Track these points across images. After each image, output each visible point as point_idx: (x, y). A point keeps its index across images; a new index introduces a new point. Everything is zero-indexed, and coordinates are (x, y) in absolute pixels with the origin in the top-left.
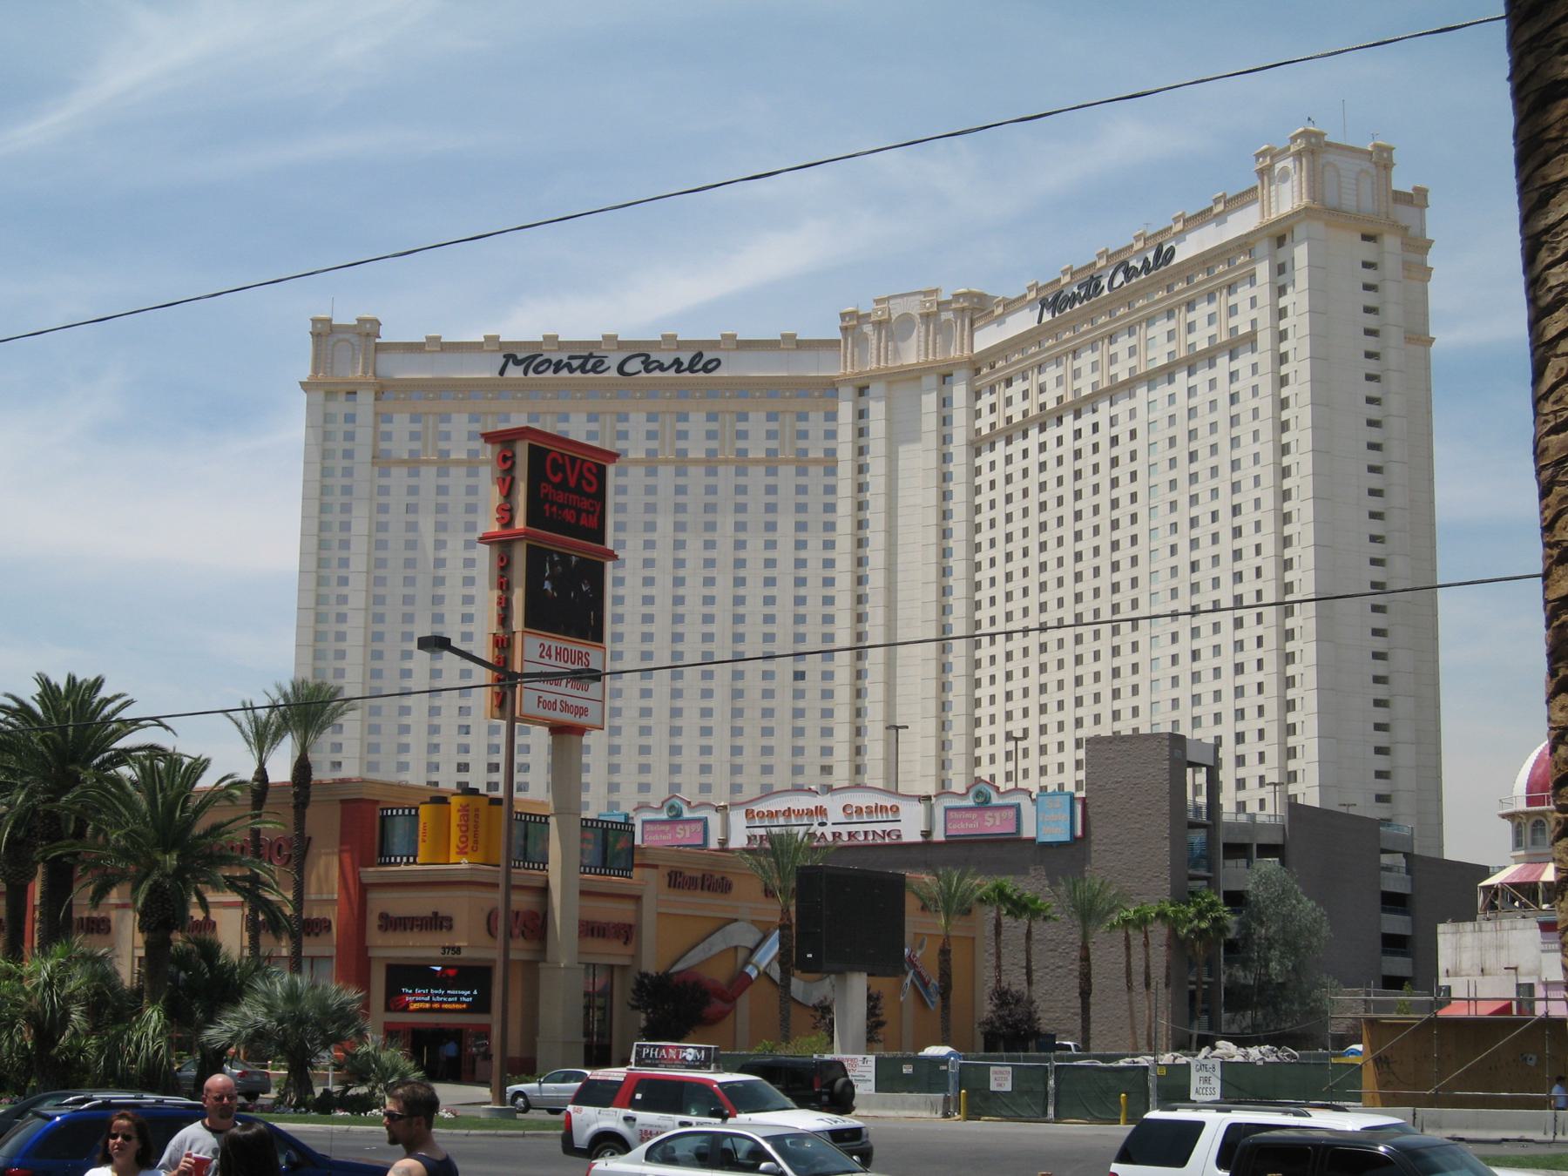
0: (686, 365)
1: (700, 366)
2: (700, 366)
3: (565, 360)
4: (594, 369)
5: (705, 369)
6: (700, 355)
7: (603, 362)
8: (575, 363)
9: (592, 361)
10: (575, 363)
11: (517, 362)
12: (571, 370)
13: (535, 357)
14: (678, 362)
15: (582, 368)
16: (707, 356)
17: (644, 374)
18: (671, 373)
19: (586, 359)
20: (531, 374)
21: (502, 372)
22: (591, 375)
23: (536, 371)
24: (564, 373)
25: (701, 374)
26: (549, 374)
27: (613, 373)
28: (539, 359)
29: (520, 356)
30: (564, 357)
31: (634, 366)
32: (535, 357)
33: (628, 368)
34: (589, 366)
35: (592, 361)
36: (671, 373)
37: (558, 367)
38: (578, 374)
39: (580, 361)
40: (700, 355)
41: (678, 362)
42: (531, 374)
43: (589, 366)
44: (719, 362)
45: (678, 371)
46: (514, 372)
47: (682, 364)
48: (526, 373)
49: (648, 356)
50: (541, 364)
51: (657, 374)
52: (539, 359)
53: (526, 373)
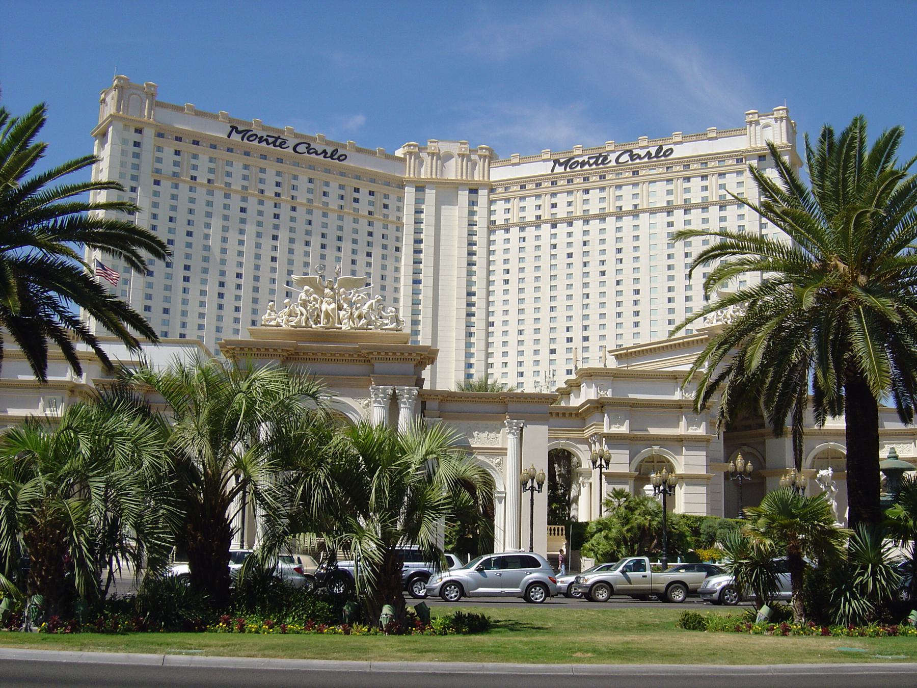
0: (653, 155)
1: (662, 154)
2: (662, 154)
3: (586, 160)
4: (603, 163)
5: (664, 155)
6: (661, 148)
7: (607, 159)
8: (592, 161)
9: (601, 159)
10: (592, 161)
11: (560, 165)
12: (590, 165)
13: (569, 160)
14: (649, 153)
15: (596, 163)
16: (665, 148)
17: (630, 162)
18: (646, 160)
19: (597, 158)
20: (568, 169)
21: (552, 171)
22: (601, 166)
23: (570, 168)
24: (587, 167)
25: (663, 158)
26: (579, 168)
27: (613, 163)
28: (573, 161)
29: (562, 161)
30: (586, 158)
31: (625, 158)
32: (569, 160)
33: (620, 161)
34: (600, 162)
35: (601, 159)
36: (646, 160)
37: (583, 164)
38: (594, 166)
39: (594, 160)
40: (661, 148)
41: (649, 153)
42: (568, 169)
43: (600, 162)
44: (672, 150)
45: (649, 158)
46: (559, 169)
47: (651, 154)
48: (565, 169)
49: (631, 151)
50: (574, 163)
51: (638, 161)
52: (573, 161)
53: (565, 169)
